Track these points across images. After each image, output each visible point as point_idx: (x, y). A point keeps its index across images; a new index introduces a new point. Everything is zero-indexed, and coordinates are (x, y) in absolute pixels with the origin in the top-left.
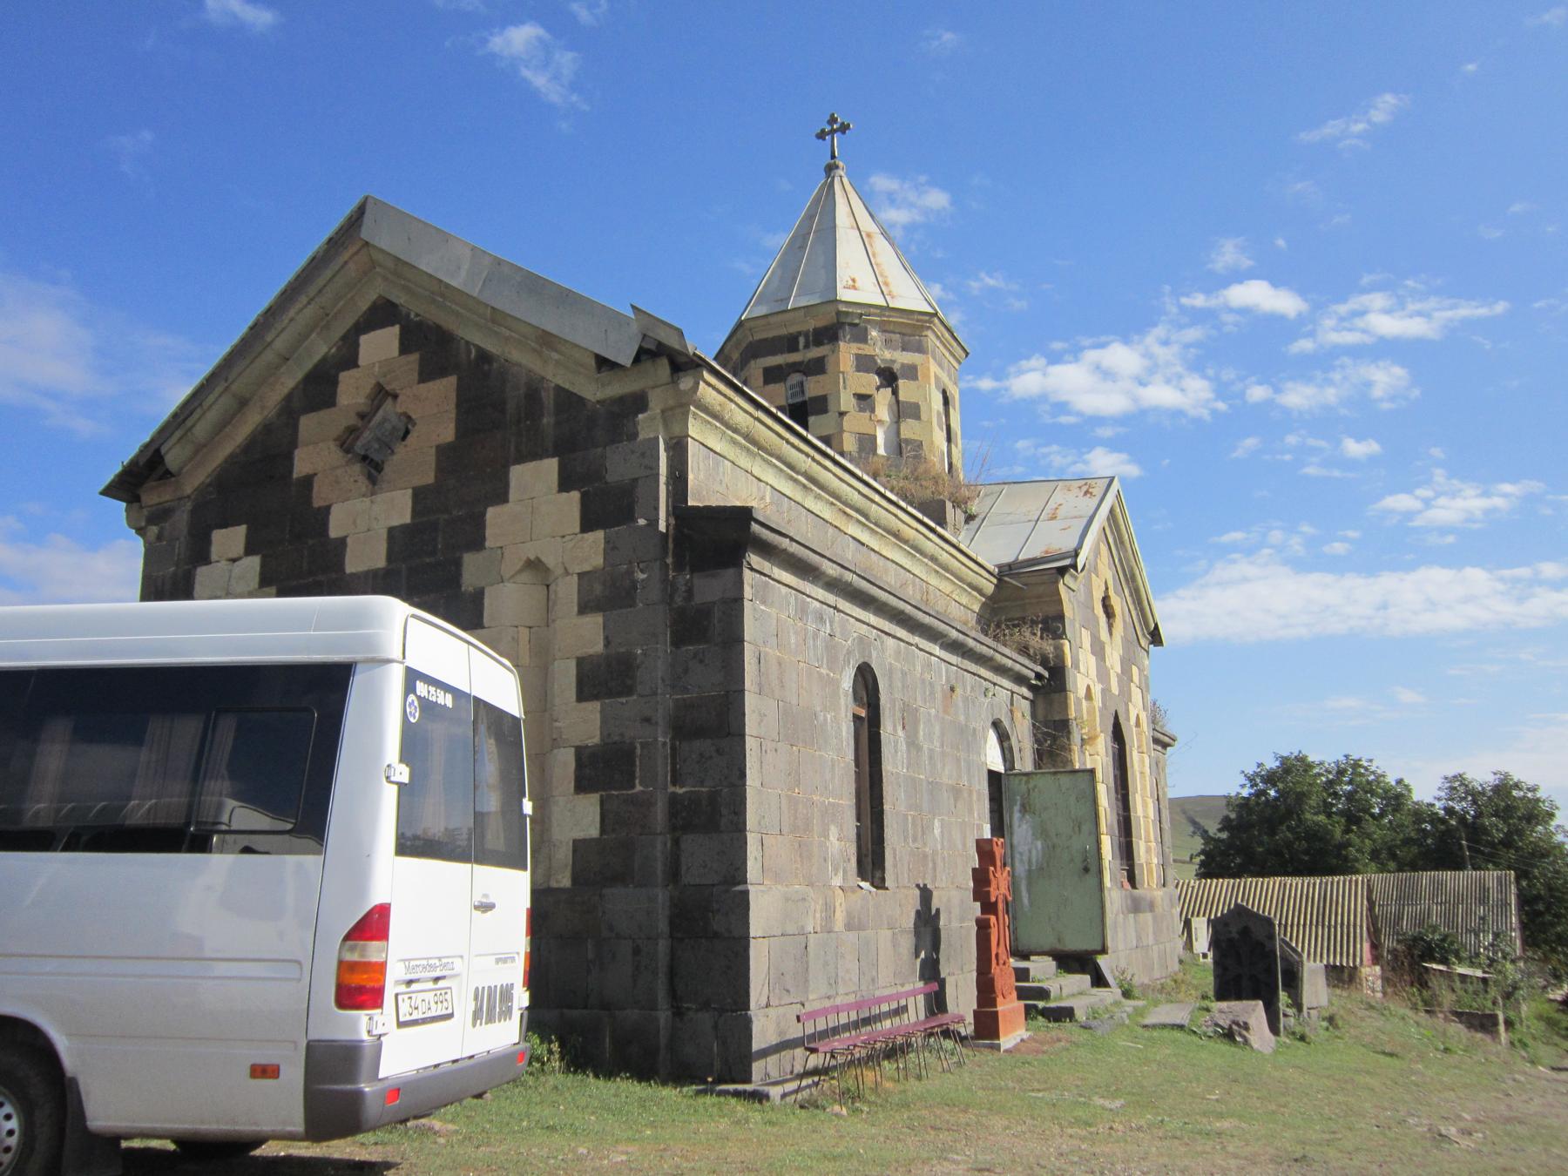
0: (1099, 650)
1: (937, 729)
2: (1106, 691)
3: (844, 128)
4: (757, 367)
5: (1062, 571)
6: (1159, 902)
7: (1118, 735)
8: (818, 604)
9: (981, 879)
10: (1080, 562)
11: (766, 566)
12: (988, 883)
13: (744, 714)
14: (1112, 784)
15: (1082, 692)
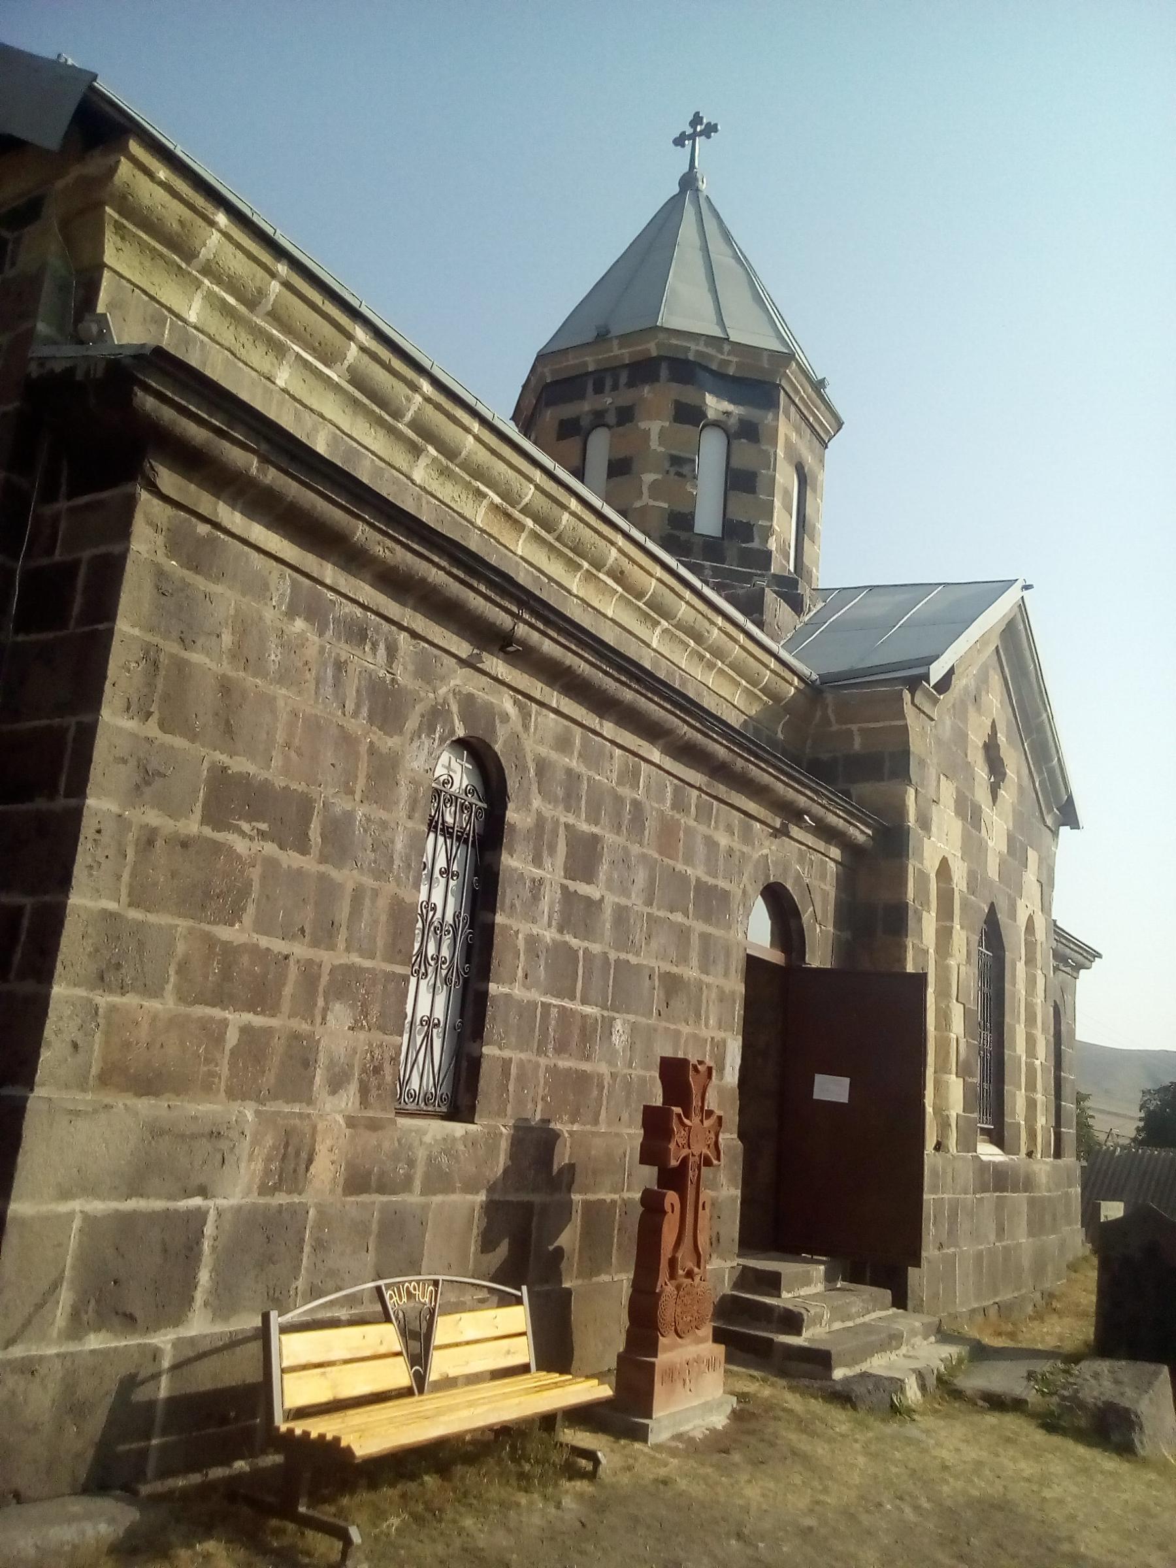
0: (970, 814)
1: (641, 876)
2: (972, 877)
3: (711, 129)
4: (549, 417)
5: (915, 683)
6: (1043, 1179)
7: (992, 935)
8: (358, 611)
9: (656, 1125)
10: (937, 672)
11: (205, 502)
12: (668, 1134)
13: (90, 761)
14: (975, 1006)
15: (931, 865)
